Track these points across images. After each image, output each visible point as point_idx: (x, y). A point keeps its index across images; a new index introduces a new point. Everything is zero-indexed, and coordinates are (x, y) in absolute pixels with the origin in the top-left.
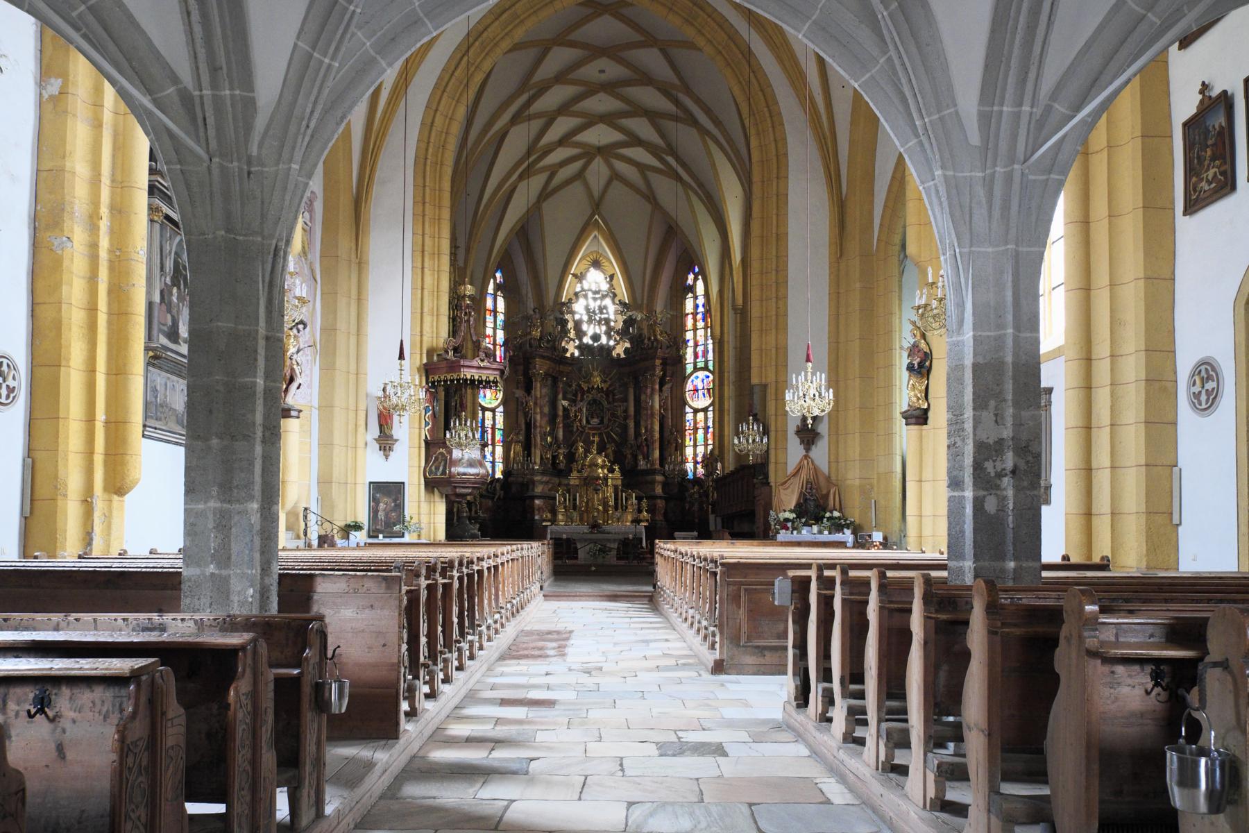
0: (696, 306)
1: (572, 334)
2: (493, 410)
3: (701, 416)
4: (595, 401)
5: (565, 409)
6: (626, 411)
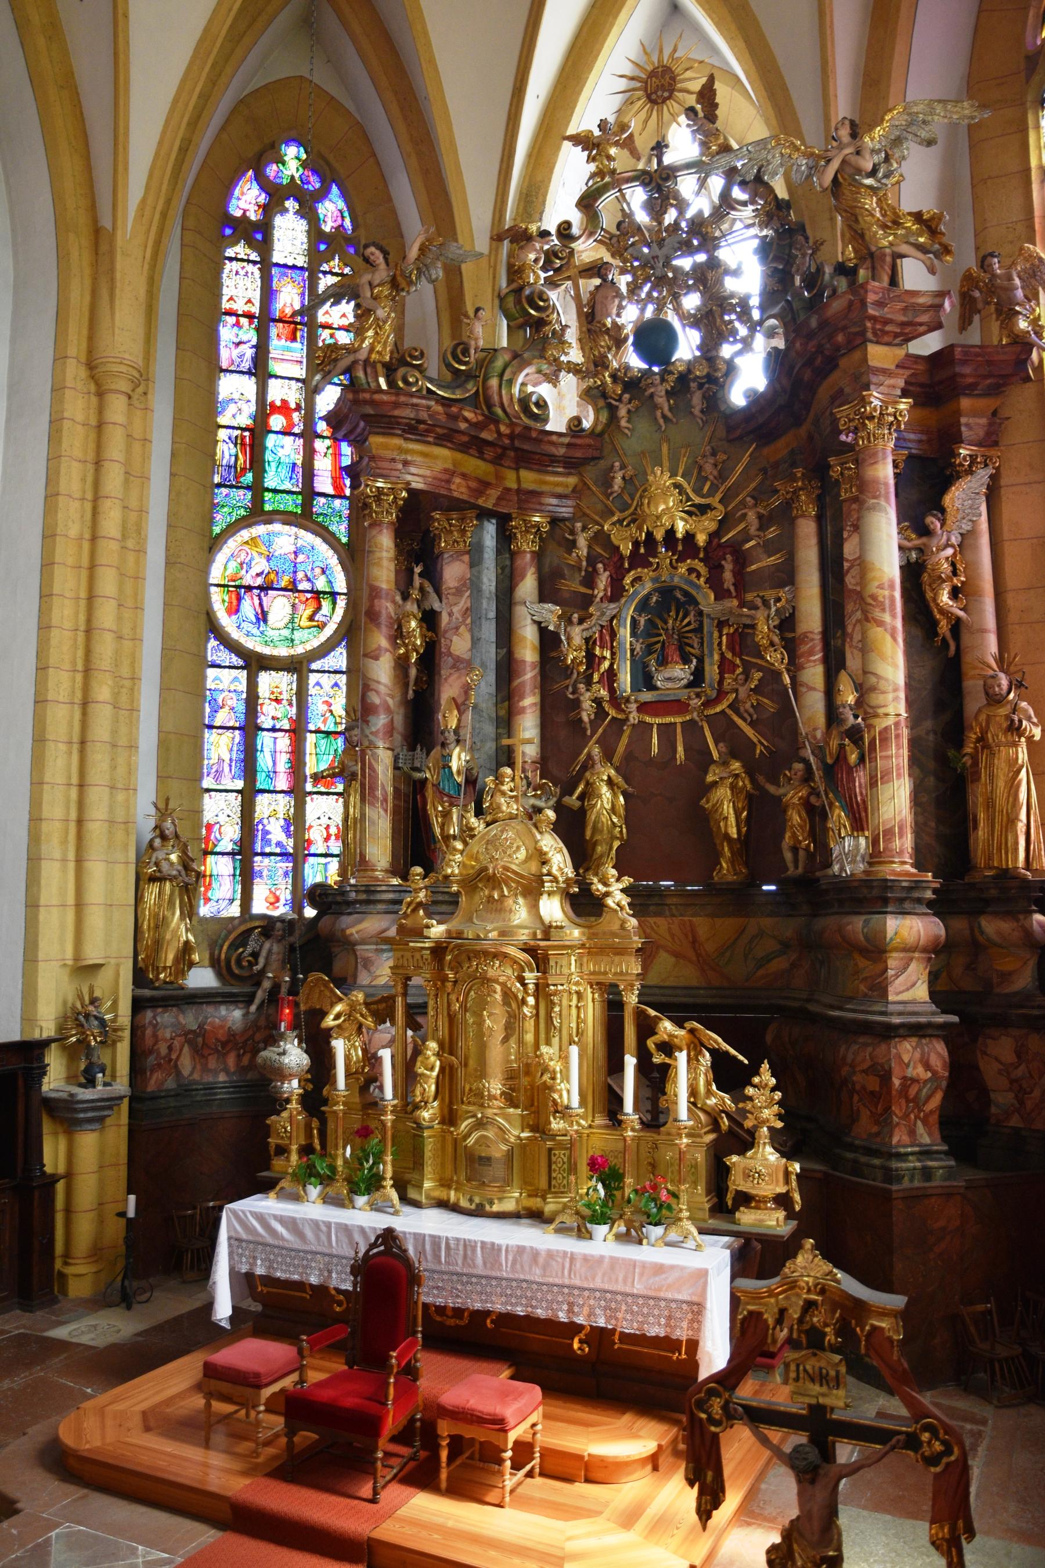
2: (297, 666)
4: (666, 592)
5: (548, 641)
6: (787, 623)
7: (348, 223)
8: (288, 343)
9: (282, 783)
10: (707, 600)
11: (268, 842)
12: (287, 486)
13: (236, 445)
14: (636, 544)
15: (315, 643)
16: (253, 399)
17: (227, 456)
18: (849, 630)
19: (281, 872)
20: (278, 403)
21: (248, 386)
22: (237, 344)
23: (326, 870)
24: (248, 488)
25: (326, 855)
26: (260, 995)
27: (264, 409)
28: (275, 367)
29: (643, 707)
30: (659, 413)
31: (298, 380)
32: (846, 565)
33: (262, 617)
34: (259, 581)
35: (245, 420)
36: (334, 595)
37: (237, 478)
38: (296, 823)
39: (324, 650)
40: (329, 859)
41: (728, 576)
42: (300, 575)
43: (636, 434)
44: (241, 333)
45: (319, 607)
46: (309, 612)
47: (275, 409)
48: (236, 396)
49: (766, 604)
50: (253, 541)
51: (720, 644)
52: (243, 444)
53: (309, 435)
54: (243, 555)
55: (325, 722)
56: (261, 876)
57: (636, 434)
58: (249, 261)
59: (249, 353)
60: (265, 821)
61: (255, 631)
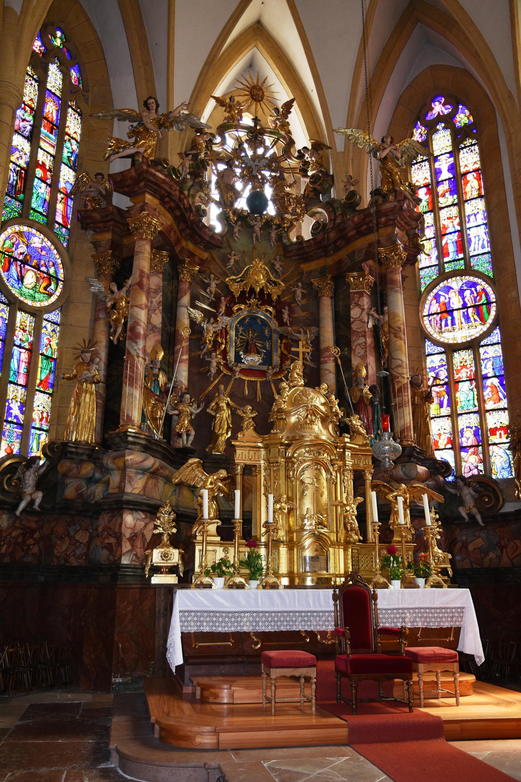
0: (436, 173)
1: (215, 195)
2: (36, 314)
3: (462, 357)
7: (81, 86)
8: (48, 133)
9: (22, 380)
10: (274, 324)
11: (10, 415)
12: (41, 210)
13: (17, 175)
14: (243, 293)
15: (46, 304)
16: (28, 154)
17: (12, 179)
18: (354, 347)
19: (15, 435)
20: (40, 163)
21: (26, 146)
22: (24, 120)
23: (39, 438)
24: (19, 201)
25: (40, 429)
26: (22, 505)
27: (33, 162)
28: (42, 144)
29: (243, 371)
30: (254, 235)
31: (51, 155)
32: (352, 320)
33: (21, 279)
34: (21, 258)
35: (22, 163)
36: (58, 280)
37: (15, 194)
38: (26, 406)
39: (49, 309)
40: (41, 432)
41: (286, 317)
42: (42, 262)
43: (240, 241)
44: (26, 114)
45: (49, 285)
46: (44, 285)
47: (38, 165)
48: (20, 148)
49: (305, 333)
50: (20, 234)
51: (280, 347)
52: (21, 177)
53: (54, 187)
54: (14, 239)
55: (46, 350)
56: (4, 435)
57: (240, 241)
58: (34, 79)
59: (29, 128)
60: (10, 401)
61: (16, 285)
